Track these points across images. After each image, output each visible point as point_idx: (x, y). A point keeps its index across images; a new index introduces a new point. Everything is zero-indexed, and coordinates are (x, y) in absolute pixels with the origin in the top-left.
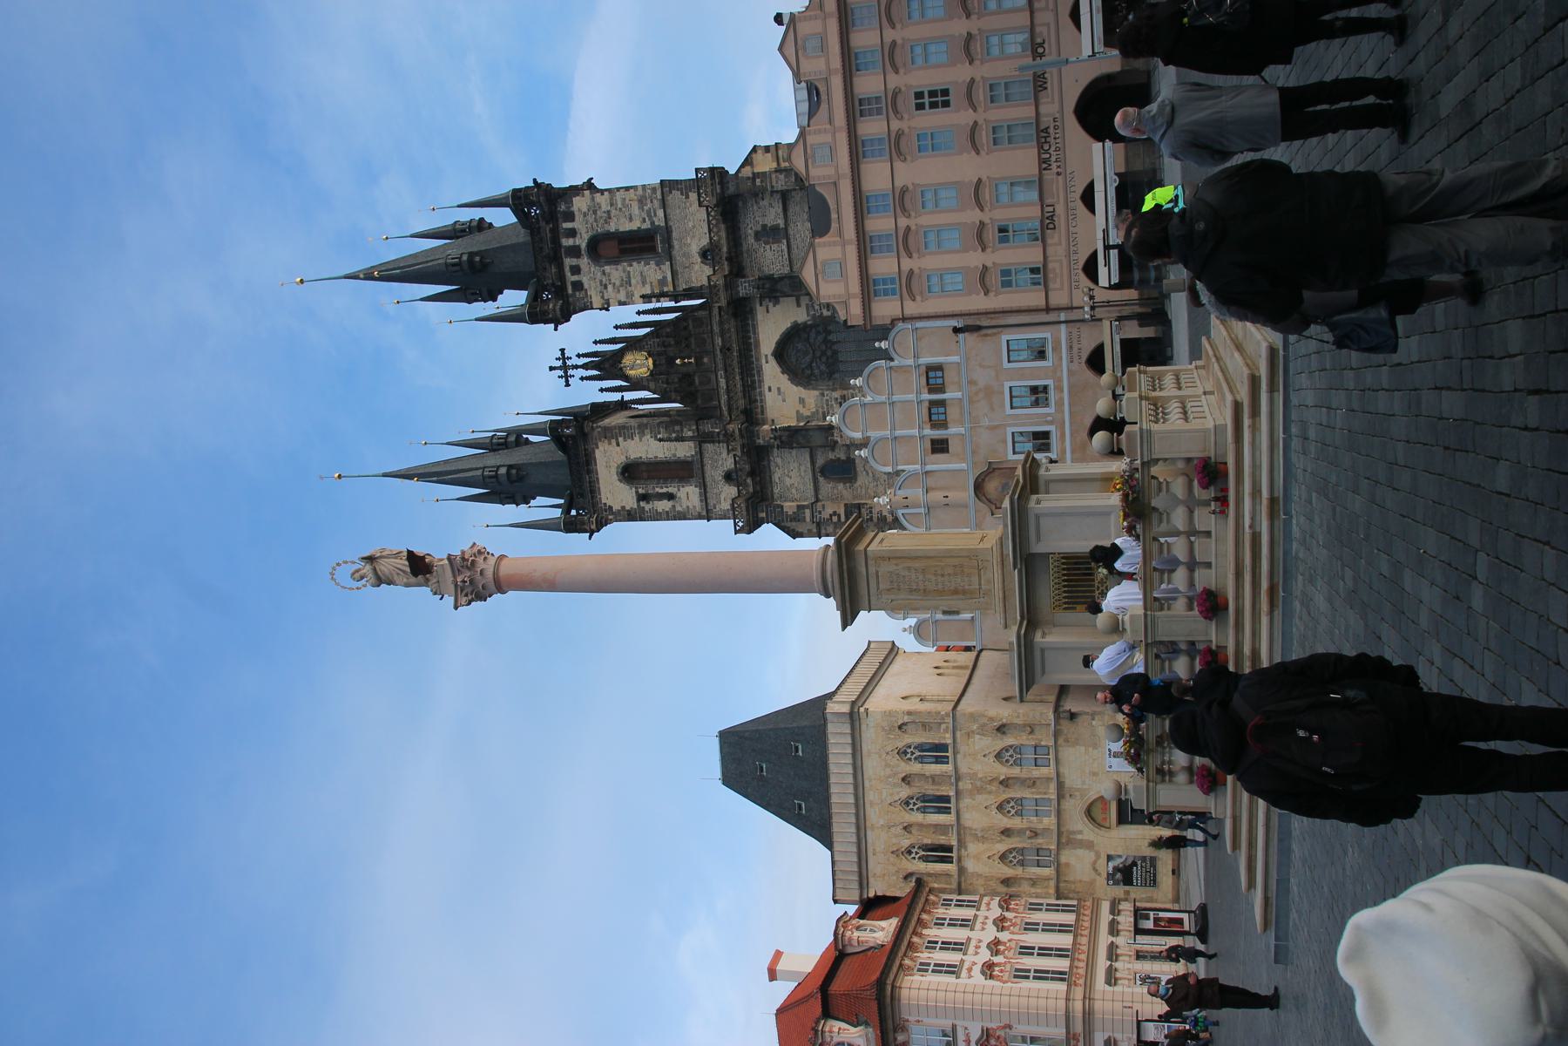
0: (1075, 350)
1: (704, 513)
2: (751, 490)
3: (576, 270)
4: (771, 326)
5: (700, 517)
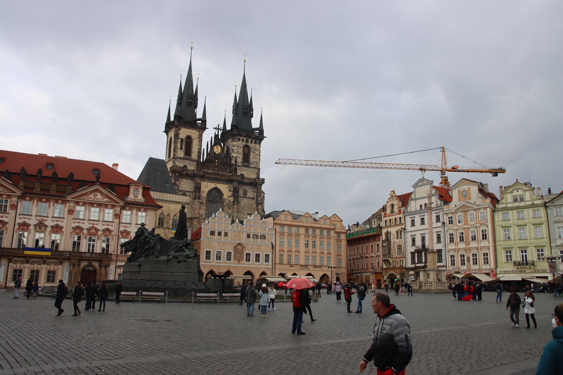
0: (267, 269)
1: (175, 157)
2: (182, 173)
3: (243, 140)
4: (224, 188)
5: (174, 155)
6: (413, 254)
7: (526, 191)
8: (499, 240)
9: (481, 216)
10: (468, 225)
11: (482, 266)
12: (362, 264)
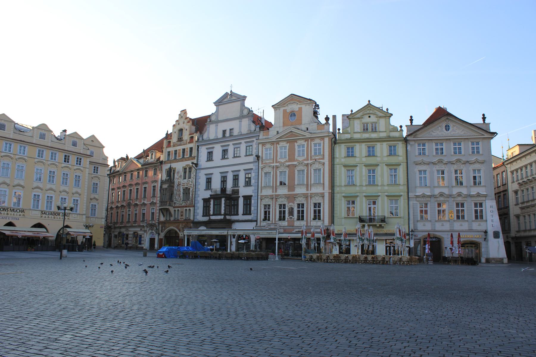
6: (206, 201)
7: (380, 117)
8: (338, 185)
9: (315, 150)
10: (294, 160)
11: (310, 222)
12: (129, 215)
